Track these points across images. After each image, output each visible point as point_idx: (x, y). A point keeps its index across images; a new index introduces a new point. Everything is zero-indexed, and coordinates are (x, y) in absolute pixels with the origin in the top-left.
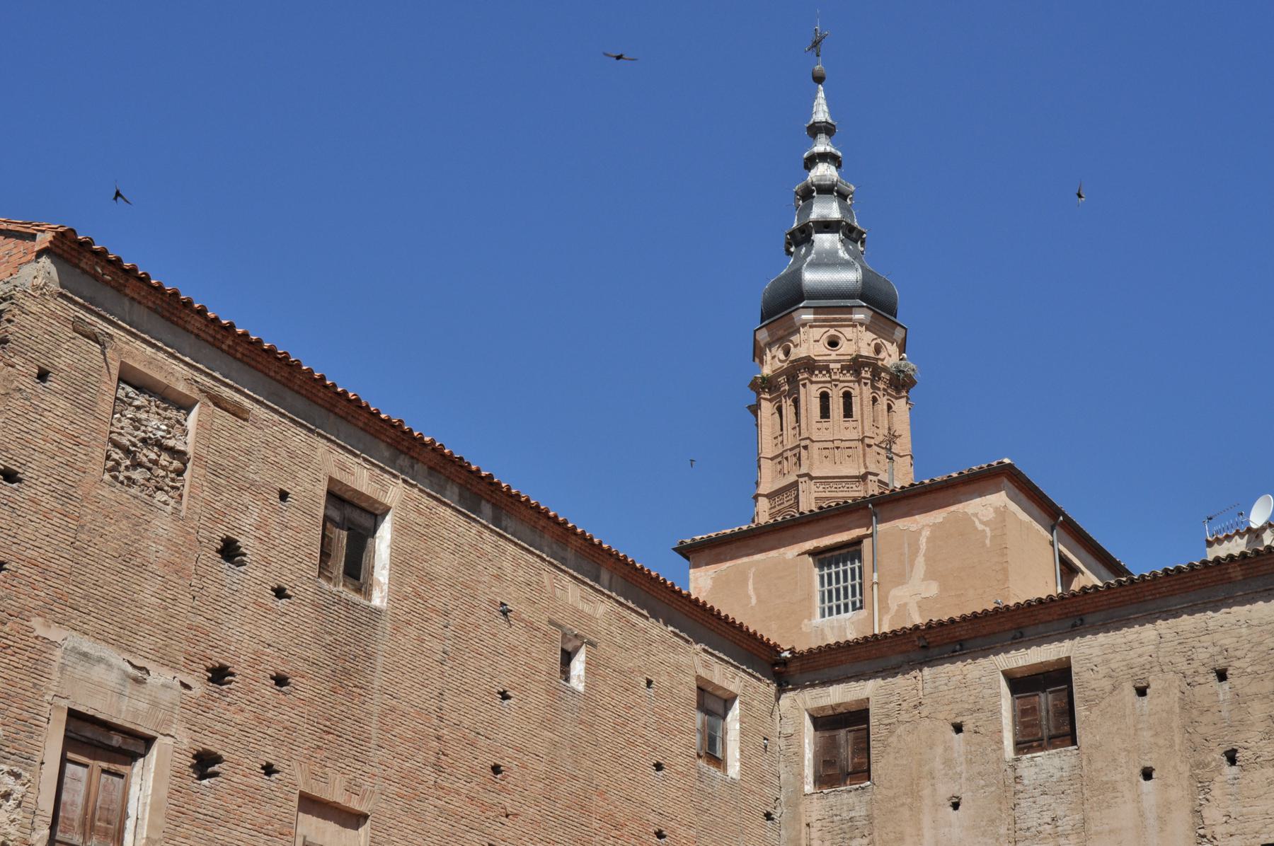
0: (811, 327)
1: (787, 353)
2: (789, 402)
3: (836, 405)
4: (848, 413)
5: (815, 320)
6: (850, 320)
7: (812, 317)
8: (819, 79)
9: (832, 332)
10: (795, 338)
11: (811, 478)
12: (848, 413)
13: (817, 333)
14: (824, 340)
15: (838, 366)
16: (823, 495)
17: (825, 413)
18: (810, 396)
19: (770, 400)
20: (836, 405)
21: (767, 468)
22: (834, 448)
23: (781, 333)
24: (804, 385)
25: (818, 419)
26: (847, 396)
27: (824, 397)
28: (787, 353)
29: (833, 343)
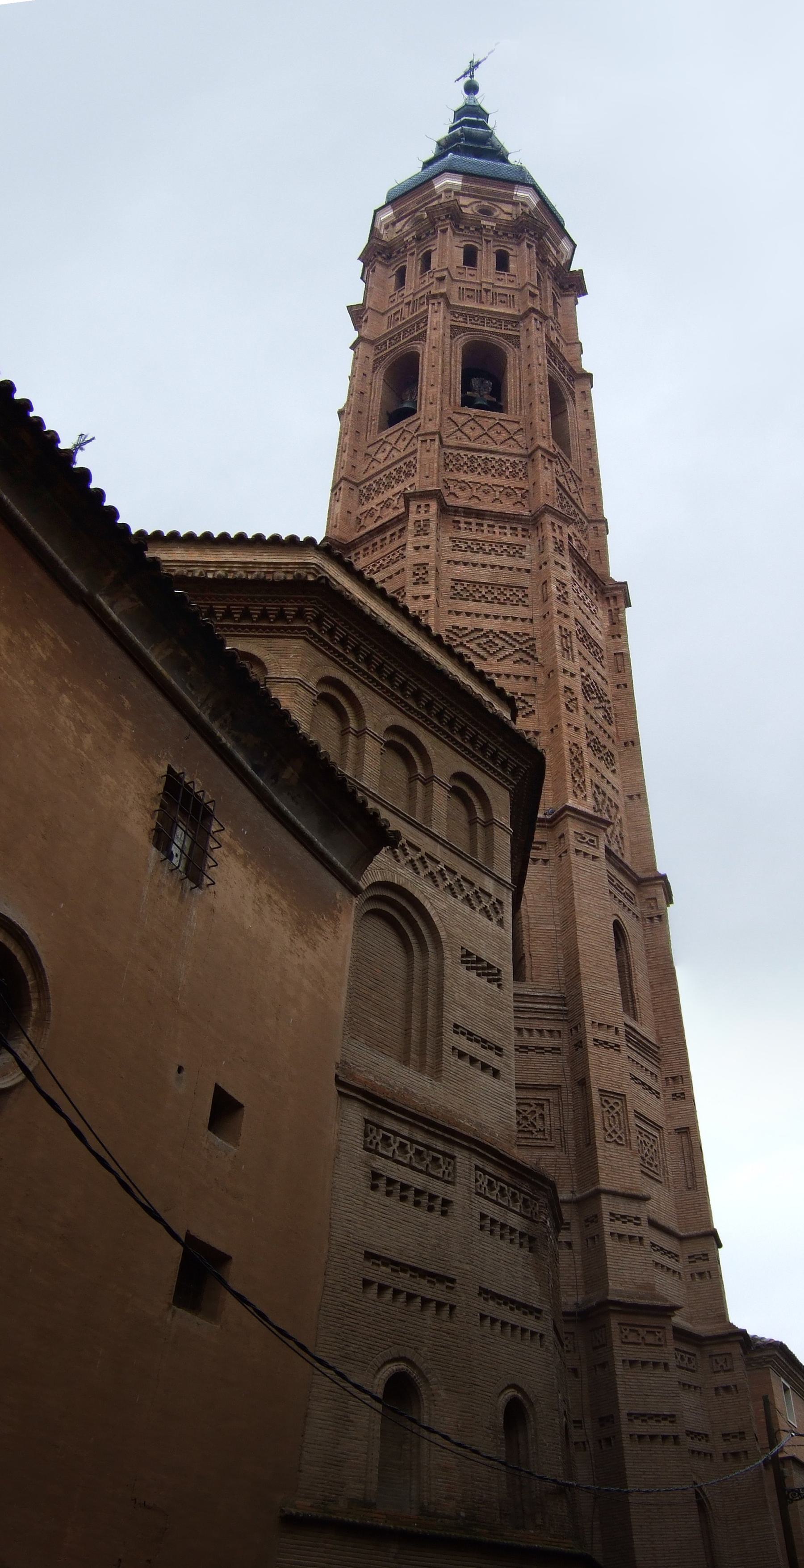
9: (486, 203)
16: (464, 325)
25: (461, 264)
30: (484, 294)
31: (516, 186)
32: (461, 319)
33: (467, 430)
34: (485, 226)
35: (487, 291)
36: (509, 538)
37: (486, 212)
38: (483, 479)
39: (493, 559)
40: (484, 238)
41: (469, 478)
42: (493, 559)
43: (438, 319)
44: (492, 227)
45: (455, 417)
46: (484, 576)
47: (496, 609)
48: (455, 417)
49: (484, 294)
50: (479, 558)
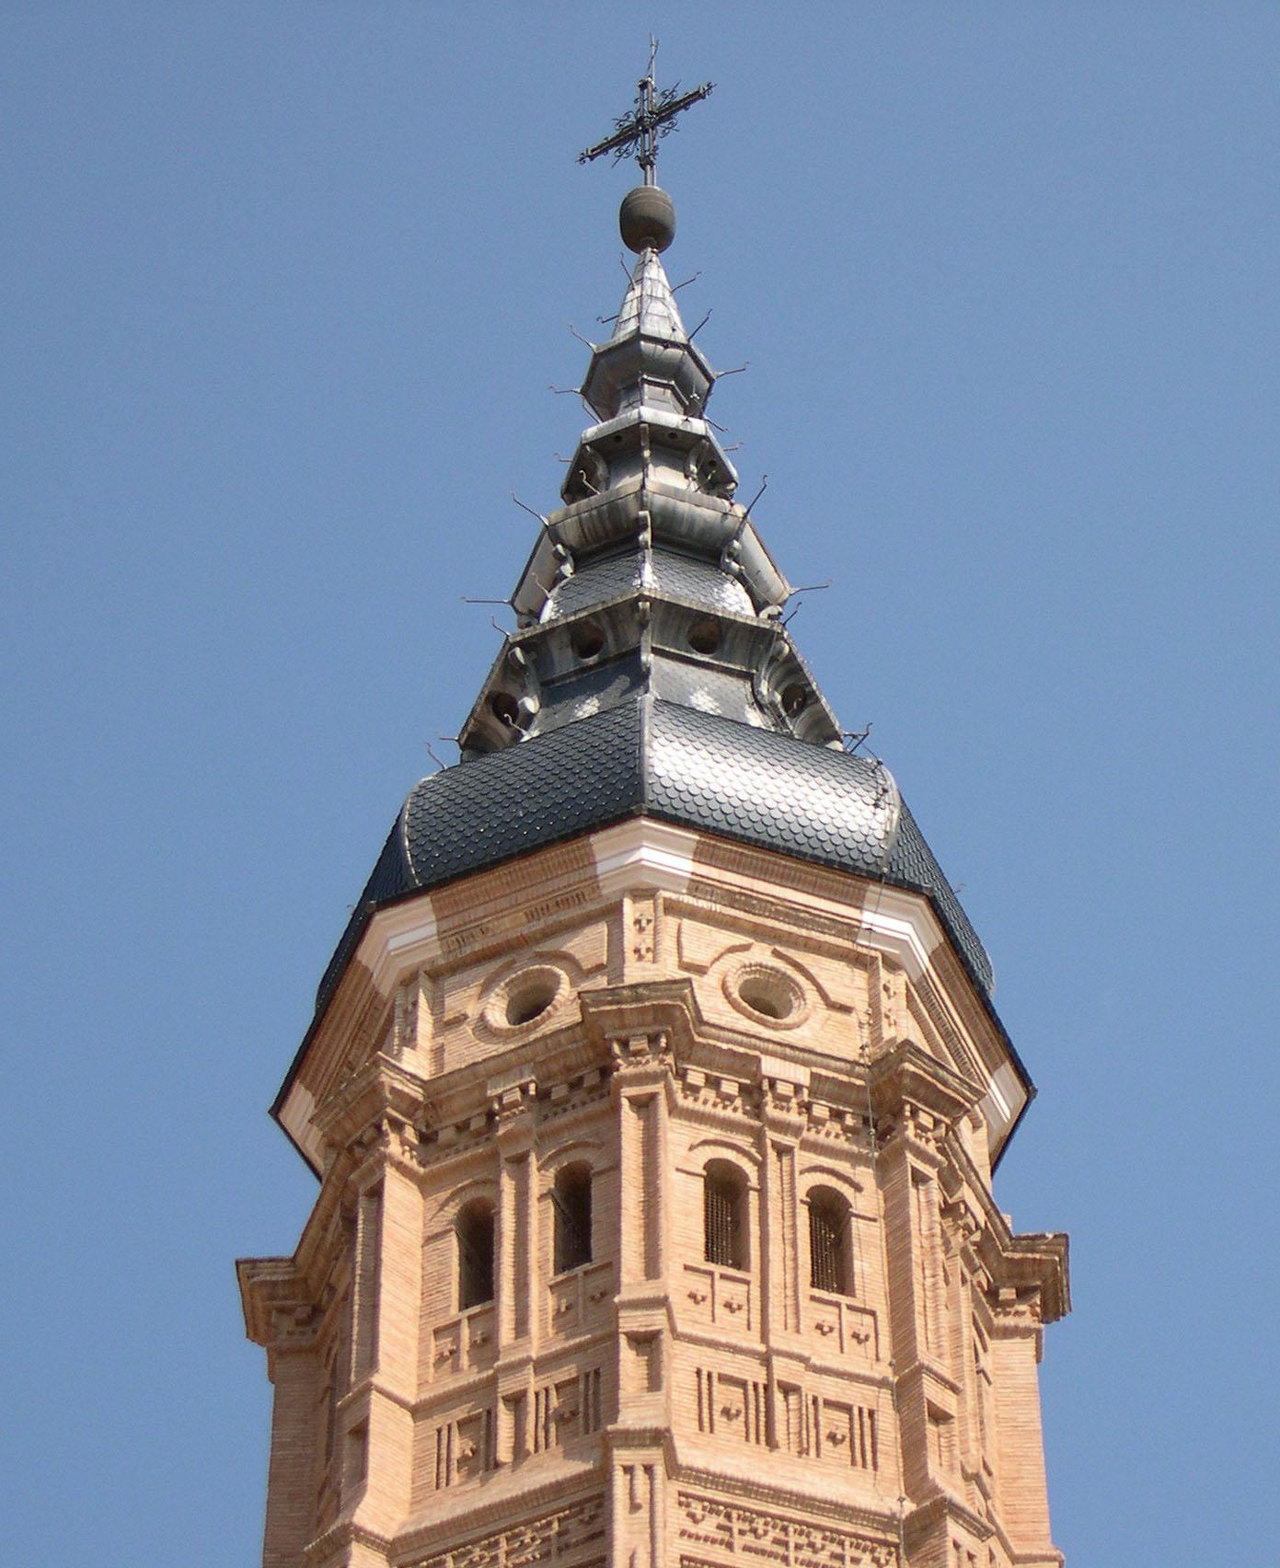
0: (672, 908)
2: (541, 1180)
3: (782, 1235)
4: (831, 1265)
5: (696, 886)
6: (850, 930)
7: (684, 865)
8: (644, 230)
9: (761, 954)
10: (588, 944)
11: (674, 1470)
12: (831, 1265)
13: (703, 942)
15: (802, 1075)
17: (726, 1234)
19: (426, 1185)
20: (782, 1235)
21: (393, 1450)
23: (510, 925)
24: (644, 1106)
25: (698, 1258)
26: (829, 1215)
27: (725, 1190)
28: (529, 1006)
30: (778, 1396)
31: (873, 889)
32: (709, 1526)
34: (772, 1083)
35: (788, 1389)
37: (766, 998)
40: (771, 1135)
44: (798, 1088)
49: (778, 1396)
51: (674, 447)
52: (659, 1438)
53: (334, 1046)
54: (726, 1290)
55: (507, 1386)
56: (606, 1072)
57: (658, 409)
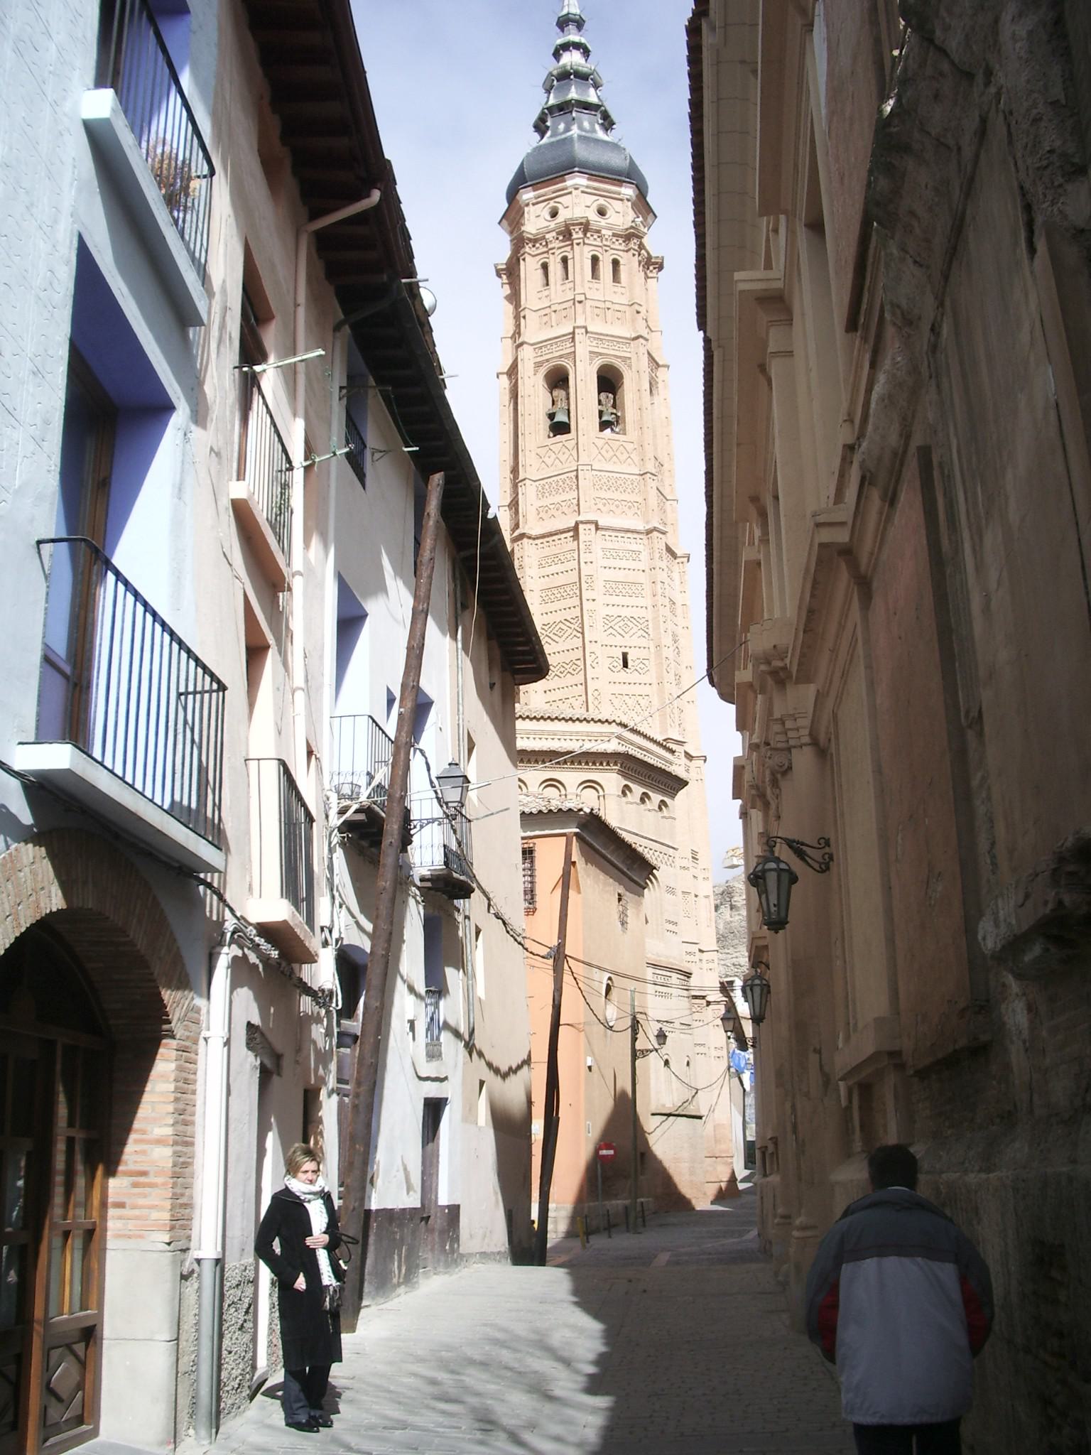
1: (554, 214)
3: (606, 269)
9: (602, 201)
14: (594, 207)
16: (596, 350)
18: (581, 257)
20: (606, 269)
22: (604, 309)
26: (616, 263)
27: (595, 260)
28: (554, 214)
29: (602, 212)
33: (603, 452)
36: (634, 547)
38: (616, 495)
39: (624, 564)
41: (608, 495)
42: (624, 564)
43: (583, 347)
45: (596, 441)
46: (620, 576)
47: (627, 601)
48: (596, 441)
50: (618, 563)
51: (577, 46)
52: (585, 328)
53: (513, 214)
54: (596, 286)
55: (554, 308)
56: (571, 235)
57: (574, 37)
